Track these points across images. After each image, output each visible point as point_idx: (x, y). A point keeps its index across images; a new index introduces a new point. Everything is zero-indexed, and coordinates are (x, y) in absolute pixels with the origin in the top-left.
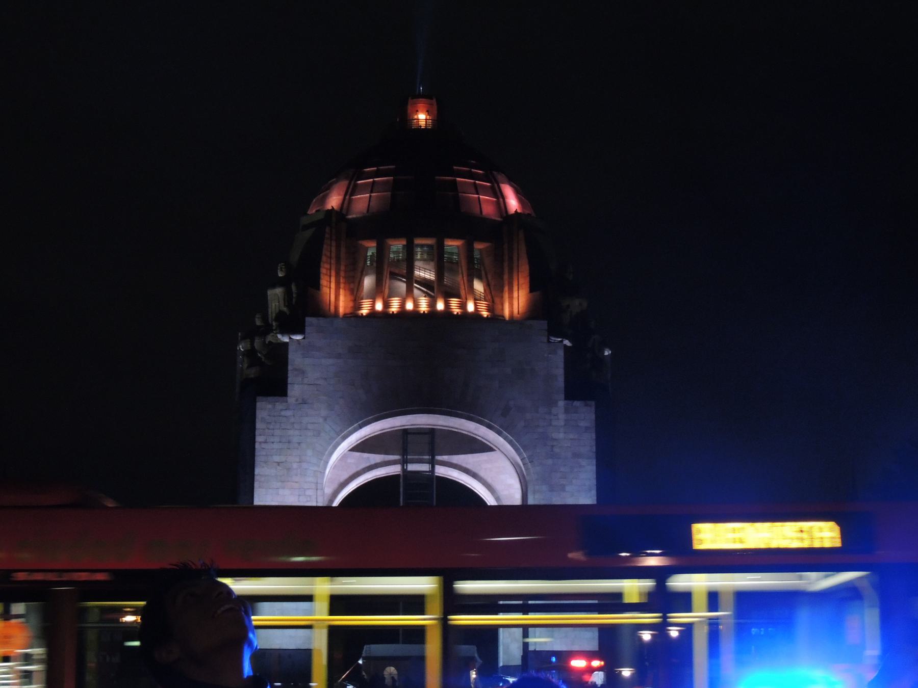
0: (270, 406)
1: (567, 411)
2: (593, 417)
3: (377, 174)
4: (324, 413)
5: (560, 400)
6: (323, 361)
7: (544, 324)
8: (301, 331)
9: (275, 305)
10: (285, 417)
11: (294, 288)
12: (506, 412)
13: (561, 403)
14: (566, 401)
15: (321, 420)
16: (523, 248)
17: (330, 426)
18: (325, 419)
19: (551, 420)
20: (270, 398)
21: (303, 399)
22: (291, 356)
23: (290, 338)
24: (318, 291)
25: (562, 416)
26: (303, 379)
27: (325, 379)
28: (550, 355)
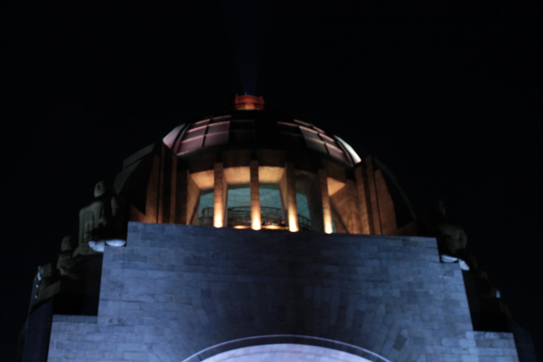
0: (71, 327)
1: (479, 344)
2: (515, 352)
3: (211, 122)
4: (148, 338)
5: (468, 330)
6: (150, 273)
7: (432, 242)
8: (122, 235)
9: (88, 225)
10: (92, 342)
11: (113, 203)
12: (399, 343)
13: (471, 334)
14: (476, 333)
15: (145, 348)
16: (383, 187)
17: (158, 357)
18: (150, 347)
19: (460, 355)
20: (73, 318)
21: (120, 320)
22: (105, 265)
23: (106, 245)
24: (141, 215)
25: (474, 351)
26: (120, 295)
27: (153, 296)
28: (446, 277)
